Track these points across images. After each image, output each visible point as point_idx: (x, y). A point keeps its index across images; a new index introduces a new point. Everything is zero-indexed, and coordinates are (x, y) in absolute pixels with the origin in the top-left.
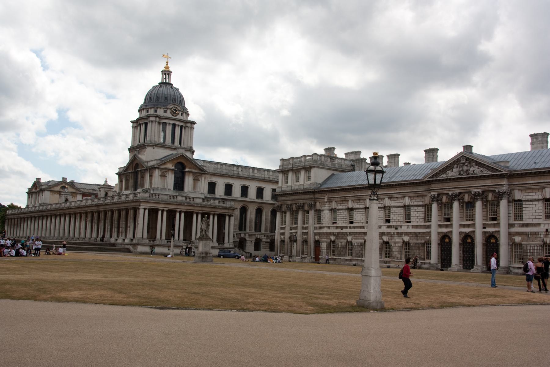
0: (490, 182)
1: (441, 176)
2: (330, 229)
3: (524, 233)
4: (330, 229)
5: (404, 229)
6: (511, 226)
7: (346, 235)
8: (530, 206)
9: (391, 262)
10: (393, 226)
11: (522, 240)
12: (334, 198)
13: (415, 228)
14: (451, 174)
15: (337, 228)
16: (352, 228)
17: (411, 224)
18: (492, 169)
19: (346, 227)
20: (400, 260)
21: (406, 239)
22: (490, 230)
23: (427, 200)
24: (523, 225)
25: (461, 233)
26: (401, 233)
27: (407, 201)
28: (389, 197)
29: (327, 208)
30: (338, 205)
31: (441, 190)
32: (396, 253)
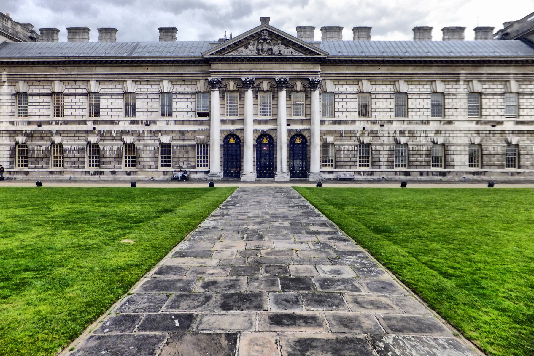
0: (300, 68)
1: (229, 54)
2: (13, 124)
3: (337, 132)
4: (13, 124)
5: (161, 126)
6: (322, 122)
7: (49, 135)
8: (344, 100)
9: (139, 172)
10: (142, 121)
11: (335, 140)
12: (22, 76)
13: (179, 124)
14: (244, 52)
15: (29, 123)
16: (61, 124)
17: (174, 118)
18: (305, 50)
19: (49, 123)
20: (156, 170)
21: (166, 139)
22: (298, 127)
23: (201, 86)
24: (335, 123)
25: (222, 131)
26: (157, 132)
27: (166, 86)
28: (134, 79)
29: (7, 91)
30: (31, 87)
31: (228, 73)
32: (148, 160)
